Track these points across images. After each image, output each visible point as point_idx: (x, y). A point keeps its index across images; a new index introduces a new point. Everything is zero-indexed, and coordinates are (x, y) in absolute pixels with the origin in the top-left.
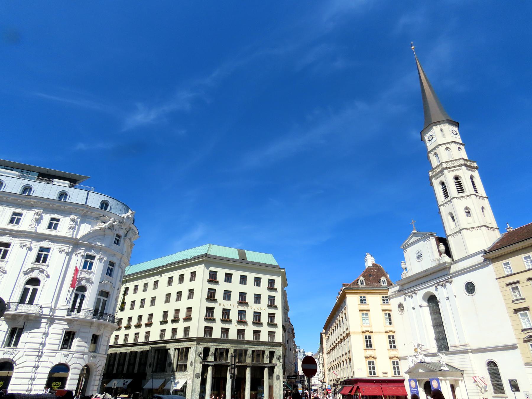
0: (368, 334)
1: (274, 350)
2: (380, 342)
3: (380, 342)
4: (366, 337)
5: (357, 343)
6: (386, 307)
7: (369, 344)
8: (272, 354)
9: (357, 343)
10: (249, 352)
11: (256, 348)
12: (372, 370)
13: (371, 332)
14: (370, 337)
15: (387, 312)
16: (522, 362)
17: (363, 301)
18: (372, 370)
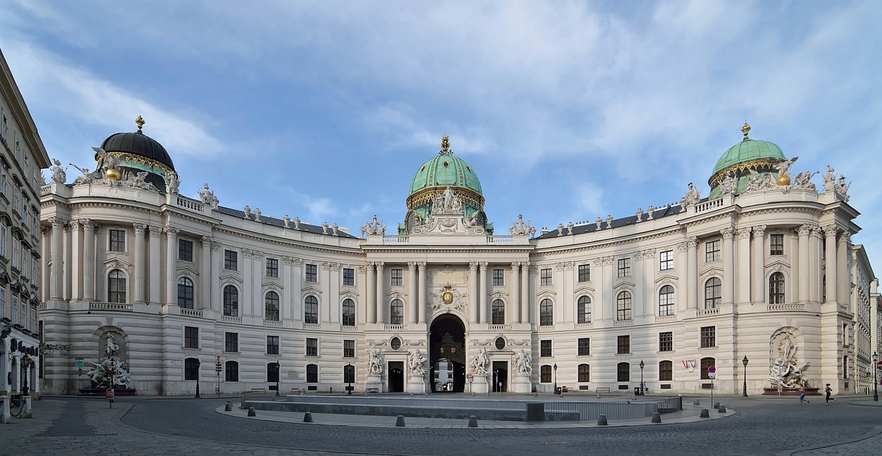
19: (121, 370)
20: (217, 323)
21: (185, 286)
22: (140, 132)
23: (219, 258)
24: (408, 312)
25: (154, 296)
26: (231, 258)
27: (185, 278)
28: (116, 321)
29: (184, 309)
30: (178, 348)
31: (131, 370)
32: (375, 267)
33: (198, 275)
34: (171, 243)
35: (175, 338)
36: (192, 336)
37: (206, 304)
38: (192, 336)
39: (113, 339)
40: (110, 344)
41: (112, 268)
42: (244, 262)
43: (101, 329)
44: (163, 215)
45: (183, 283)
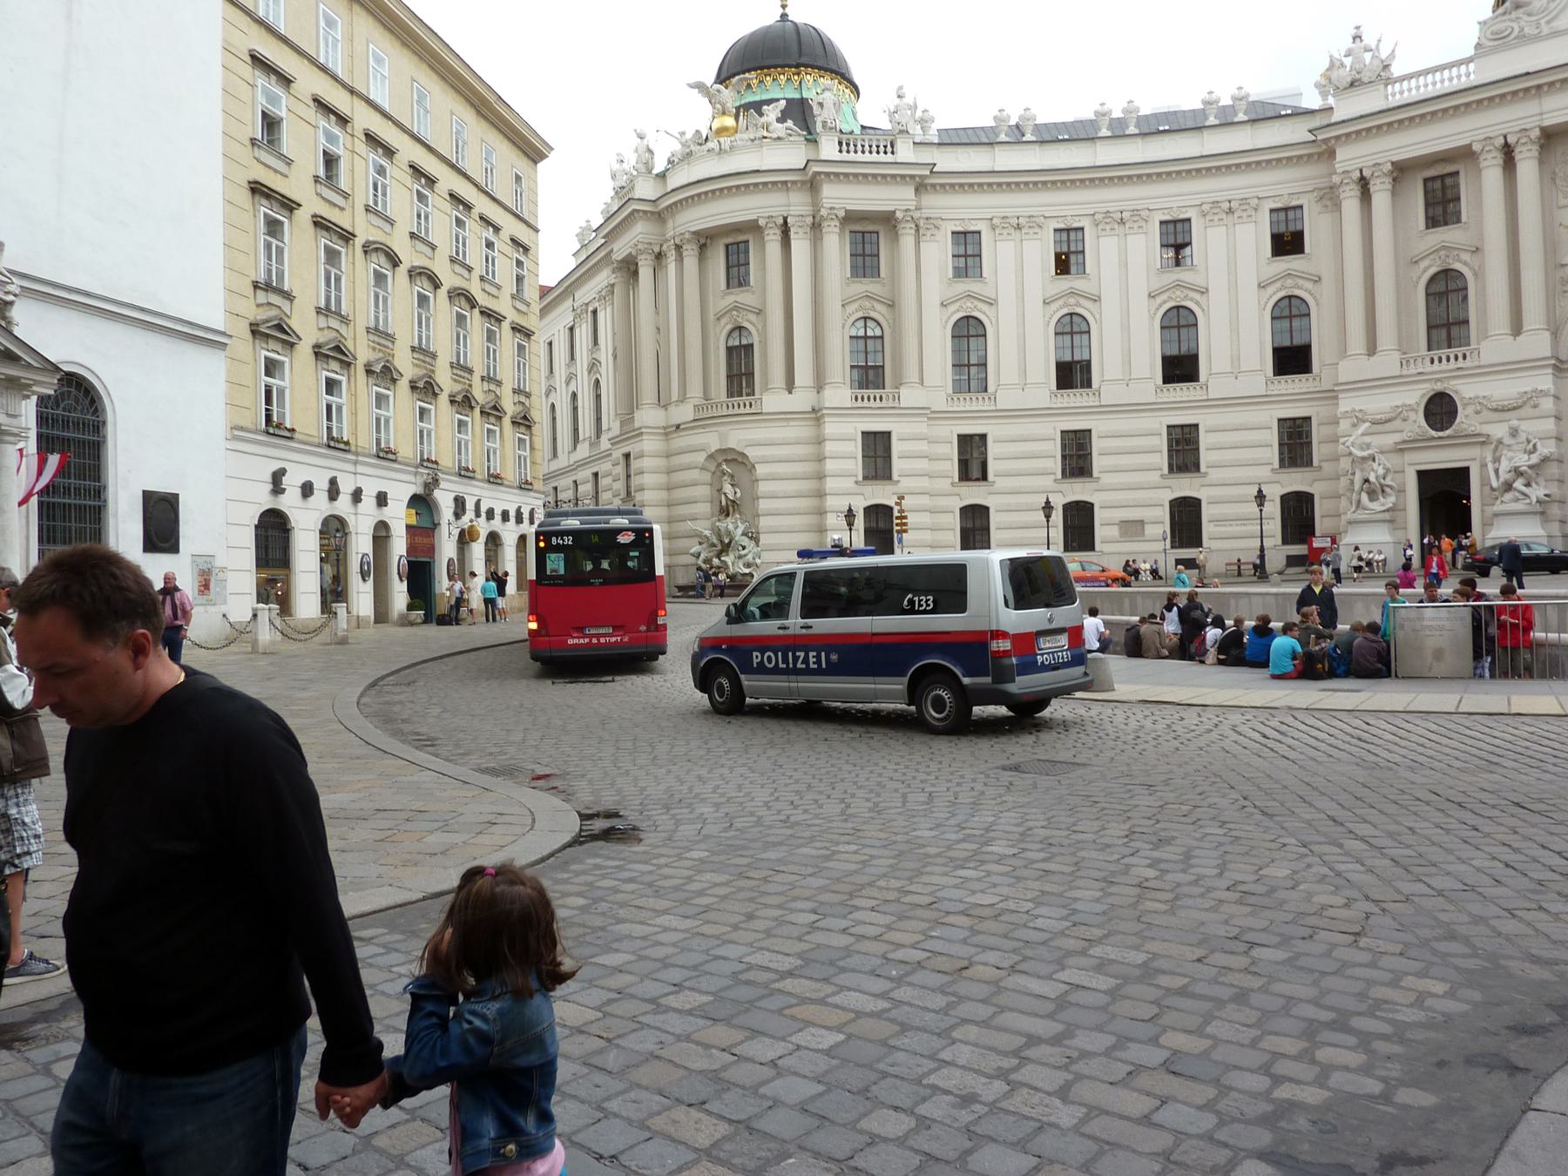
19: (745, 541)
20: (933, 415)
21: (866, 337)
22: (784, 16)
23: (938, 254)
24: (1488, 299)
25: (803, 374)
26: (967, 252)
27: (865, 318)
28: (738, 437)
29: (860, 392)
30: (848, 484)
31: (764, 539)
32: (1364, 183)
33: (892, 305)
34: (836, 247)
35: (846, 458)
36: (877, 449)
37: (911, 373)
38: (877, 449)
39: (732, 476)
40: (728, 488)
41: (729, 327)
42: (998, 253)
43: (711, 457)
44: (812, 185)
45: (861, 333)
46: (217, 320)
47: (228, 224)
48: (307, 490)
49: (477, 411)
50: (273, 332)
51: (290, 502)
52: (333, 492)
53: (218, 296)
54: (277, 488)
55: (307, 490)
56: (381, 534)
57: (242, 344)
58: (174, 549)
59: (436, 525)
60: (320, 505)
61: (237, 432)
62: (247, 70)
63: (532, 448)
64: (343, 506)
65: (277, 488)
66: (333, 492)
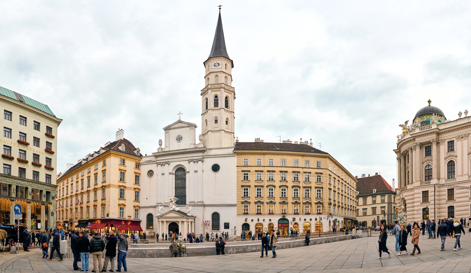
0: (122, 188)
1: (50, 191)
2: (130, 195)
3: (130, 195)
4: (121, 190)
5: (113, 194)
6: (137, 171)
7: (122, 195)
8: (48, 193)
9: (113, 194)
10: (30, 190)
11: (36, 186)
12: (122, 213)
13: (125, 187)
14: (123, 190)
15: (137, 175)
16: (236, 214)
17: (123, 162)
18: (122, 213)
46: (235, 203)
47: (237, 191)
48: (252, 220)
49: (301, 204)
50: (246, 203)
51: (249, 222)
52: (258, 220)
53: (236, 200)
54: (246, 221)
55: (252, 220)
56: (271, 226)
57: (240, 205)
58: (228, 228)
59: (288, 223)
60: (256, 222)
61: (238, 215)
62: (242, 173)
63: (323, 207)
64: (261, 221)
65: (246, 221)
66: (258, 220)
